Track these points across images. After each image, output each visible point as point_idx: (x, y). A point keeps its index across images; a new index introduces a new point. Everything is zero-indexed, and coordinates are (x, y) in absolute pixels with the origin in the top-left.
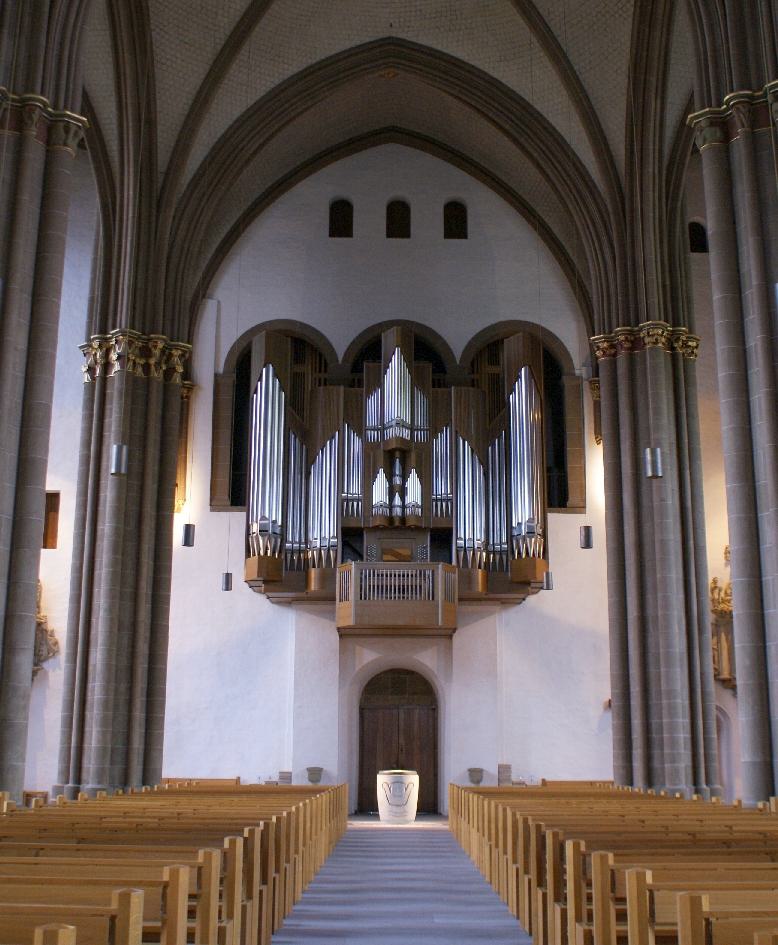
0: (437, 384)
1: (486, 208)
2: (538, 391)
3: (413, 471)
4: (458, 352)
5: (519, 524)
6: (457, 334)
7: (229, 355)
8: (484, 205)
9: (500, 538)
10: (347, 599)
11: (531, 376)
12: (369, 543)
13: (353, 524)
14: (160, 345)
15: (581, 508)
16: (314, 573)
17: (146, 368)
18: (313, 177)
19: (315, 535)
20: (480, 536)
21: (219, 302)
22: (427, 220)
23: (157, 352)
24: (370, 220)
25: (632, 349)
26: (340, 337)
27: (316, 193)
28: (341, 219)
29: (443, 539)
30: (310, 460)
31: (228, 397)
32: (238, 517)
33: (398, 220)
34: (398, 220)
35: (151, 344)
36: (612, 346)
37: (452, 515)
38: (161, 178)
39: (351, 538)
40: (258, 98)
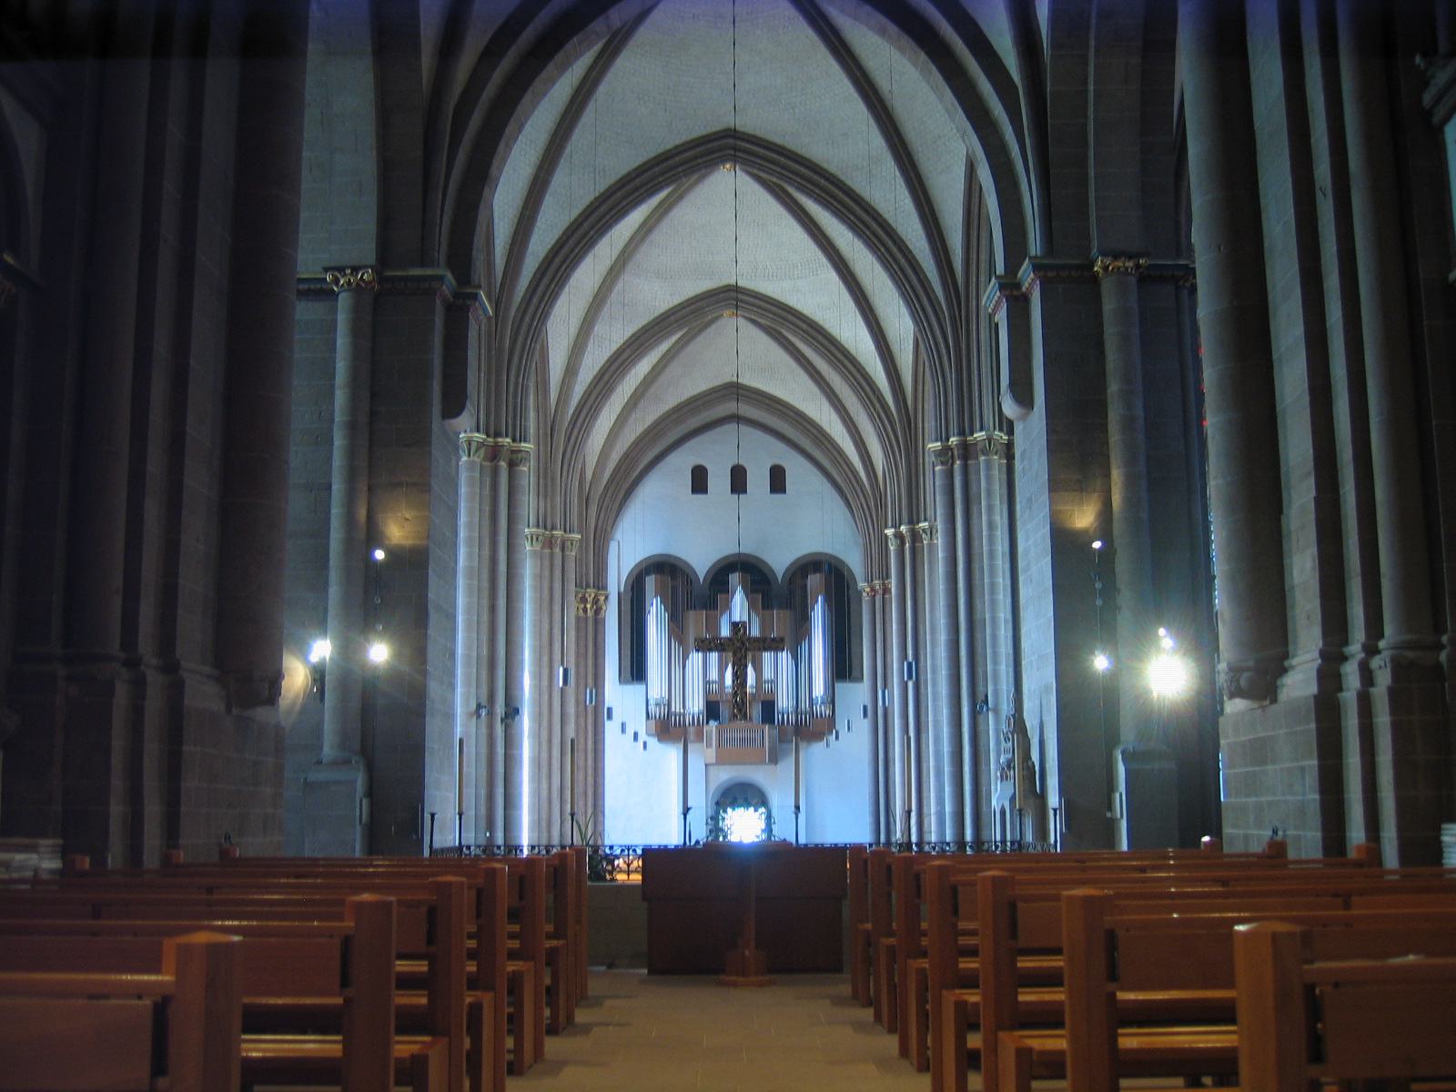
0: (764, 607)
1: (799, 472)
2: (830, 609)
3: (750, 665)
4: (780, 574)
5: (817, 698)
6: (779, 561)
7: (628, 577)
8: (798, 471)
9: (805, 705)
10: (711, 745)
11: (827, 600)
12: (725, 711)
13: (712, 698)
14: (593, 595)
15: (860, 679)
16: (691, 730)
17: (585, 610)
18: (680, 449)
19: (689, 703)
20: (792, 703)
21: (619, 543)
22: (758, 480)
23: (590, 599)
24: (719, 481)
25: (883, 595)
26: (701, 558)
27: (681, 463)
28: (699, 481)
29: (769, 707)
30: (685, 657)
31: (627, 607)
32: (640, 688)
33: (738, 481)
34: (738, 481)
35: (587, 595)
36: (873, 589)
37: (773, 693)
38: (588, 485)
39: (712, 710)
40: (646, 426)
